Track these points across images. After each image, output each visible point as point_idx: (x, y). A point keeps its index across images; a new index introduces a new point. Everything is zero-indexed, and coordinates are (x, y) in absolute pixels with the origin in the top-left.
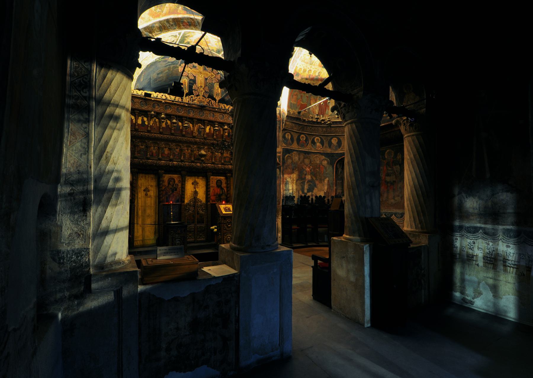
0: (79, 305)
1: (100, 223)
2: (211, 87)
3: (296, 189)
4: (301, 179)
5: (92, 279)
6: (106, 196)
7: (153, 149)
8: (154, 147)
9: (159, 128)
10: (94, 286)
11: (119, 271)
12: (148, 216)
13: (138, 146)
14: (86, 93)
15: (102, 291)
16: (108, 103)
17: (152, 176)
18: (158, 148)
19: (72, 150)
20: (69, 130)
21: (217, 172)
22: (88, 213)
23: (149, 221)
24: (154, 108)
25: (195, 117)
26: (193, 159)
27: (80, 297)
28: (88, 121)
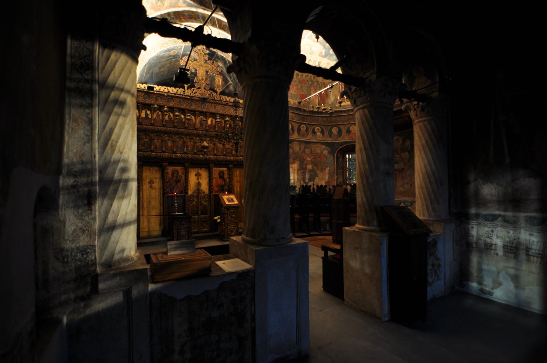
0: (86, 307)
2: (213, 79)
3: (298, 179)
4: (302, 169)
5: (99, 278)
6: (112, 188)
7: (157, 142)
9: (162, 121)
10: (101, 286)
11: (128, 269)
14: (88, 75)
15: (110, 291)
16: (113, 87)
17: (156, 168)
18: (162, 140)
19: (75, 138)
20: (70, 116)
21: (219, 164)
22: (93, 207)
23: (154, 212)
24: (157, 101)
26: (195, 151)
27: (87, 298)
28: (91, 106)
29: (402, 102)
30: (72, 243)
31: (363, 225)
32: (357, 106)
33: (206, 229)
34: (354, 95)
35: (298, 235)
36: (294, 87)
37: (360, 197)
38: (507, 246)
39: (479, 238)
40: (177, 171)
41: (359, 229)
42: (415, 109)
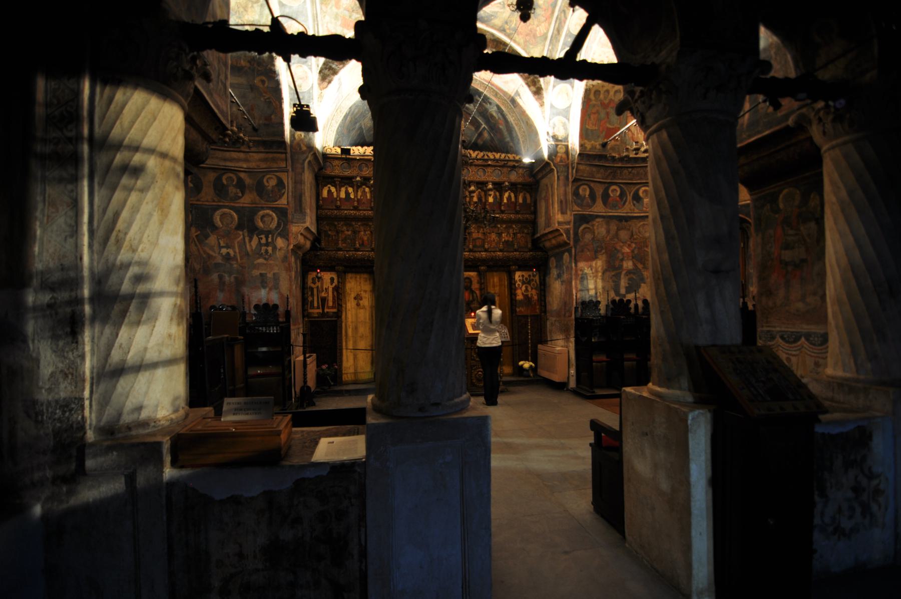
0: (71, 493)
1: (108, 355)
3: (603, 288)
4: (613, 269)
5: (87, 451)
6: (117, 308)
8: (365, 231)
10: (90, 463)
12: (362, 337)
13: (343, 232)
14: (71, 131)
15: (102, 474)
16: (118, 146)
17: (366, 276)
23: (363, 344)
24: (361, 171)
28: (75, 179)
29: (777, 106)
30: (49, 393)
31: (660, 386)
35: (599, 392)
36: (592, 117)
37: (656, 326)
42: (820, 120)
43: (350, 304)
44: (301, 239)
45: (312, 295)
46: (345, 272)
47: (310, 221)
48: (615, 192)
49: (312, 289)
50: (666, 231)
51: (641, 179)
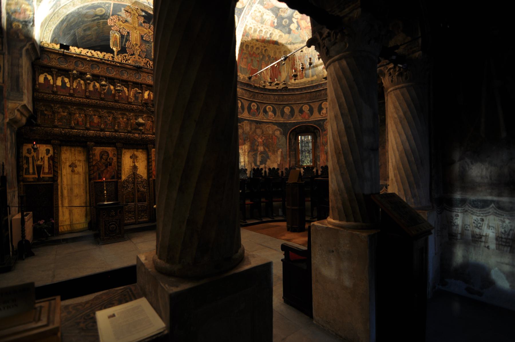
3: (248, 161)
4: (253, 150)
8: (80, 114)
12: (77, 196)
17: (79, 149)
18: (85, 115)
24: (77, 66)
25: (129, 79)
26: (129, 129)
31: (340, 220)
32: (330, 57)
33: (145, 219)
34: (326, 42)
35: (249, 222)
37: (334, 182)
38: (502, 238)
39: (464, 228)
40: (107, 153)
41: (334, 224)
42: (390, 74)
43: (65, 171)
44: (18, 115)
45: (28, 162)
46: (60, 145)
47: (27, 100)
48: (254, 106)
49: (27, 158)
50: (345, 123)
51: (267, 101)
